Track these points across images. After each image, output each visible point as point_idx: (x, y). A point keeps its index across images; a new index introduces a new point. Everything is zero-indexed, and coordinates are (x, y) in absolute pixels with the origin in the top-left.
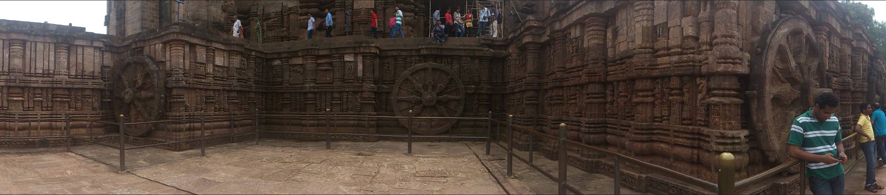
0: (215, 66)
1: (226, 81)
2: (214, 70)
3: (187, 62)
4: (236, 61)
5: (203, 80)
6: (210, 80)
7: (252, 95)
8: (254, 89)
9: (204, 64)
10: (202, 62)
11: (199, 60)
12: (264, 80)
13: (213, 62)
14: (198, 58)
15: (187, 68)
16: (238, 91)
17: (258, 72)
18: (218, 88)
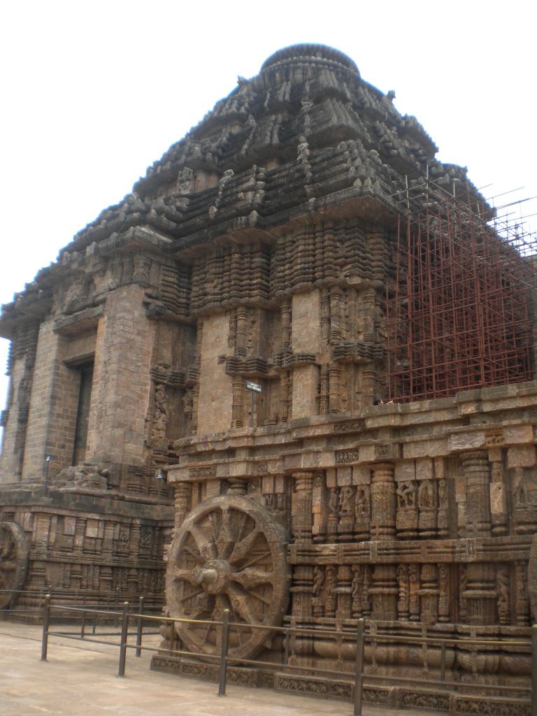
0: (86, 537)
1: (100, 555)
2: (84, 543)
3: (53, 535)
4: (112, 532)
5: (69, 554)
6: (78, 553)
7: (133, 572)
8: (135, 565)
9: (71, 536)
10: (69, 533)
11: (66, 532)
12: (155, 554)
13: (84, 533)
14: (66, 530)
15: (52, 540)
16: (112, 568)
17: (144, 544)
18: (88, 562)
